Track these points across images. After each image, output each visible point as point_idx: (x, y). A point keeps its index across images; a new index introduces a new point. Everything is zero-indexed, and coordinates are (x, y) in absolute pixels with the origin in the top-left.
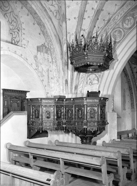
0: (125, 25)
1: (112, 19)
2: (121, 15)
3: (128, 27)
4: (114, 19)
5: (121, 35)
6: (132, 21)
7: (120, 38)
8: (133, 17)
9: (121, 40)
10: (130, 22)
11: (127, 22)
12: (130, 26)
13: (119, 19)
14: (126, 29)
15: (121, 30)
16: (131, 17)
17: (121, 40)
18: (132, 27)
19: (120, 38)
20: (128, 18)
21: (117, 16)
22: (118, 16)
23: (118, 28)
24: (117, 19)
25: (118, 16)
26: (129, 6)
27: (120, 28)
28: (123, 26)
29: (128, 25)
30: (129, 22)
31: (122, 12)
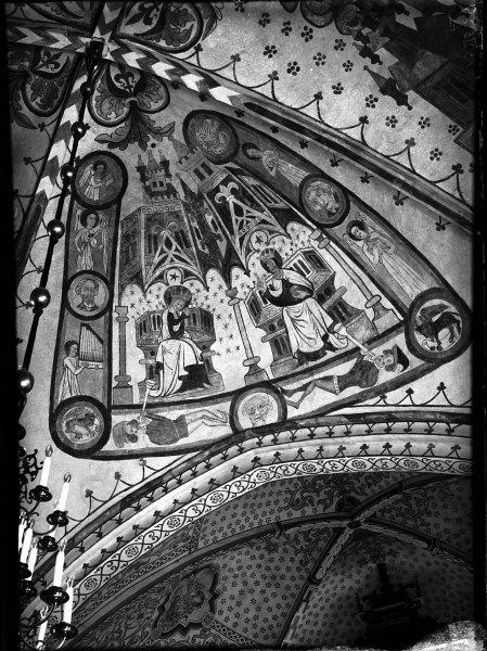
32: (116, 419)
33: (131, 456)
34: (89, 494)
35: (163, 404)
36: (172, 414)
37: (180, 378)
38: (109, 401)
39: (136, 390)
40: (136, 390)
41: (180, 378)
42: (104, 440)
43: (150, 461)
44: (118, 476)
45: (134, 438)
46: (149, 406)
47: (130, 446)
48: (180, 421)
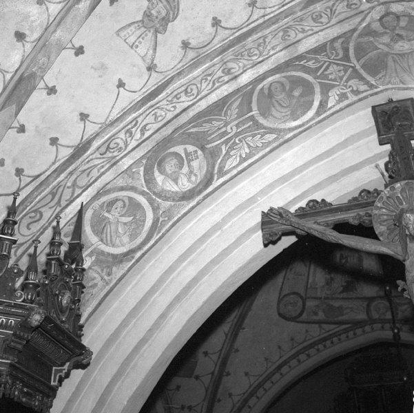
0: (159, 178)
1: (95, 144)
2: (143, 130)
3: (175, 188)
4: (108, 148)
5: (140, 223)
6: (195, 164)
7: (133, 237)
8: (203, 148)
9: (139, 247)
10: (185, 169)
11: (170, 166)
12: (185, 185)
13: (130, 148)
14: (166, 199)
15: (142, 200)
16: (191, 148)
17: (139, 247)
18: (200, 192)
19: (133, 237)
20: (179, 149)
21: (122, 135)
22: (129, 132)
23: (122, 189)
24: (122, 145)
25: (129, 132)
26: (183, 98)
27: (133, 189)
28: (150, 180)
29: (176, 181)
30: (181, 166)
31: (150, 119)
32: (310, 304)
33: (314, 323)
34: (292, 339)
35: (333, 299)
36: (336, 304)
37: (342, 286)
38: (306, 295)
39: (319, 290)
40: (319, 290)
41: (342, 286)
42: (301, 314)
43: (324, 326)
44: (307, 331)
45: (316, 314)
46: (325, 298)
47: (315, 318)
48: (340, 308)
